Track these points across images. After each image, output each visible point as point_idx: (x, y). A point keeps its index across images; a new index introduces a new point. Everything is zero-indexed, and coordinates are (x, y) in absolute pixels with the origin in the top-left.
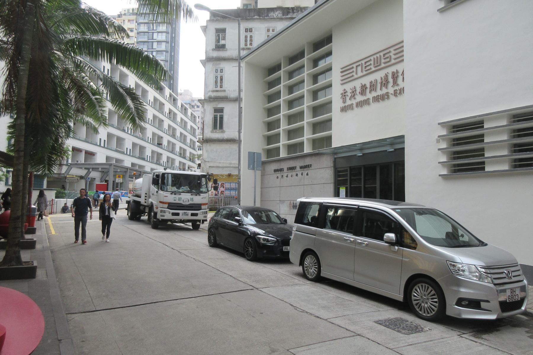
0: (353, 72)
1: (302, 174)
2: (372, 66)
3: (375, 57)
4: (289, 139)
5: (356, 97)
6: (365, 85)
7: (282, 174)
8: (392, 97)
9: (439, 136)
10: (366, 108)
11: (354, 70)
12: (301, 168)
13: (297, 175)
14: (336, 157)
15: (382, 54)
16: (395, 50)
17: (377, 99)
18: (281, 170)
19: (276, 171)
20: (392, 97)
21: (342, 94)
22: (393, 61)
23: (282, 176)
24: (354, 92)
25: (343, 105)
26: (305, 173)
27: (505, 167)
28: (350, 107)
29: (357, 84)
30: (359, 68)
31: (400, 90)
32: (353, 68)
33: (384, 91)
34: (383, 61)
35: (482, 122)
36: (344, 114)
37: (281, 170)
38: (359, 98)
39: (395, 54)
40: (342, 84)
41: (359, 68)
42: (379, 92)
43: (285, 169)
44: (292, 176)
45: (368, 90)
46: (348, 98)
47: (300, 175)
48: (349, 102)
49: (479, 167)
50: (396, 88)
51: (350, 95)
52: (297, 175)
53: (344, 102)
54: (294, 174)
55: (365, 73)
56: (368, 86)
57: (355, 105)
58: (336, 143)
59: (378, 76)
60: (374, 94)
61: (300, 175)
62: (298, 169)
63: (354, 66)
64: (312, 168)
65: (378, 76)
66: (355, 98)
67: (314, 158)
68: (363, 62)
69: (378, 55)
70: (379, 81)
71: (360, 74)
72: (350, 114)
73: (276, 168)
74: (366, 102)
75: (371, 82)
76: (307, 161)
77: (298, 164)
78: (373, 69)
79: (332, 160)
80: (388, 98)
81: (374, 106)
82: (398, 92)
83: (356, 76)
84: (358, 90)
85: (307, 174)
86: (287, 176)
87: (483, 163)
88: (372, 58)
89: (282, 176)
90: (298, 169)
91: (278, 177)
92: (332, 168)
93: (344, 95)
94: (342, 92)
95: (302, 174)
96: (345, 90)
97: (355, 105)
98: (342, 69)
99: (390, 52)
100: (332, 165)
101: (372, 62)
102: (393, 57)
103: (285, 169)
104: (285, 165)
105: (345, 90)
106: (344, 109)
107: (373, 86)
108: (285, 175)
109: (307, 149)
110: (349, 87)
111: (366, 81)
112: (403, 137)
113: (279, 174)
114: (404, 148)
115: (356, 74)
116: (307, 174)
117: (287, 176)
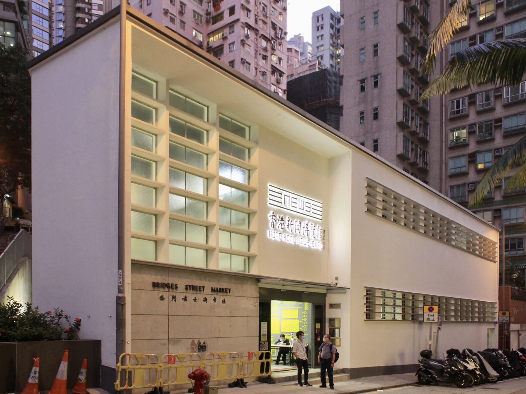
1: (215, 300)
7: (174, 294)
12: (213, 290)
13: (205, 300)
18: (169, 286)
19: (155, 285)
23: (174, 297)
37: (169, 286)
44: (195, 300)
52: (205, 300)
54: (200, 297)
62: (208, 290)
64: (231, 294)
79: (257, 289)
85: (224, 302)
86: (185, 299)
89: (174, 297)
90: (208, 290)
91: (162, 298)
95: (215, 300)
108: (180, 297)
113: (166, 293)
116: (224, 302)
117: (185, 299)
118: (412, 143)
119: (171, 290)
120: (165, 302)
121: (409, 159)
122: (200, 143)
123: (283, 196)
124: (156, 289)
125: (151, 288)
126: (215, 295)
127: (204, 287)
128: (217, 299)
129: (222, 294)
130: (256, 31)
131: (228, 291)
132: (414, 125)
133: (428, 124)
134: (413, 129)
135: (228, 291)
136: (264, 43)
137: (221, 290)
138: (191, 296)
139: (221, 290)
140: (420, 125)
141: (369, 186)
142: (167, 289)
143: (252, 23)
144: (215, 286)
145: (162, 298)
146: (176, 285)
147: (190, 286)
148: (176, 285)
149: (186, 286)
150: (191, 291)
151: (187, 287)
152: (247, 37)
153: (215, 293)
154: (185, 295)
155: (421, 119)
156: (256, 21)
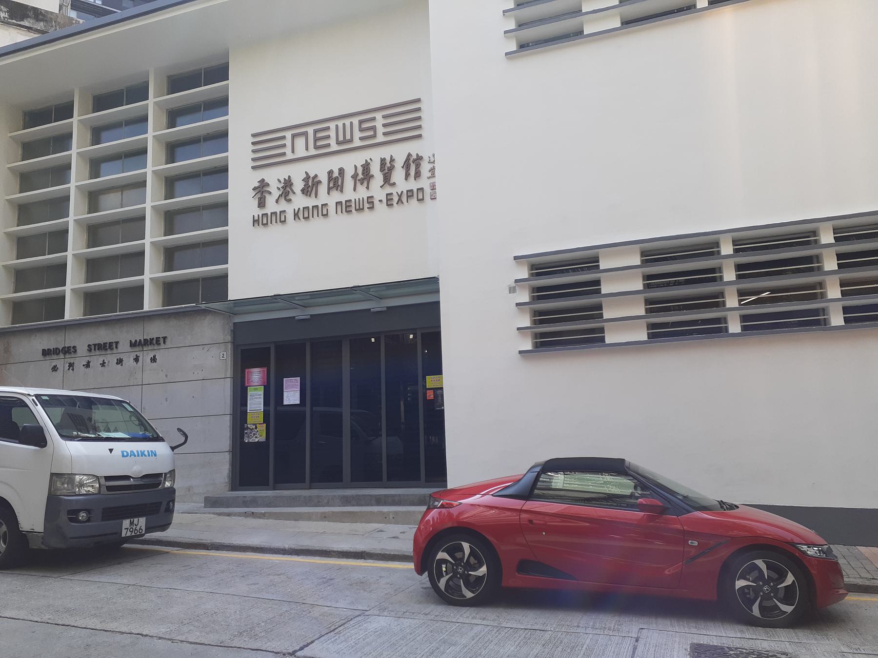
0: (284, 146)
1: (136, 360)
2: (332, 141)
3: (340, 123)
4: (89, 279)
5: (291, 196)
6: (316, 176)
8: (381, 208)
9: (516, 281)
10: (317, 222)
11: (288, 142)
12: (133, 345)
13: (120, 362)
14: (238, 320)
15: (356, 121)
16: (384, 117)
17: (346, 207)
18: (68, 351)
19: (46, 353)
20: (381, 208)
21: (254, 189)
22: (380, 138)
23: (71, 365)
24: (287, 186)
25: (260, 212)
26: (146, 356)
27: (642, 335)
28: (280, 218)
29: (297, 174)
30: (300, 142)
31: (400, 196)
32: (284, 138)
33: (363, 193)
34: (357, 134)
35: (596, 260)
36: (260, 230)
38: (300, 201)
39: (384, 125)
40: (253, 168)
41: (300, 142)
42: (349, 193)
43: (82, 349)
45: (323, 189)
46: (270, 201)
47: (129, 361)
48: (271, 206)
49: (592, 339)
50: (389, 190)
51: (276, 193)
52: (120, 362)
53: (262, 204)
54: (111, 359)
55: (313, 152)
56: (324, 178)
57: (290, 215)
58: (235, 292)
59: (350, 162)
60: (336, 196)
61: (129, 361)
62: (124, 346)
63: (288, 134)
65: (350, 162)
66: (289, 201)
67: (173, 322)
68: (310, 130)
69: (347, 122)
70: (349, 172)
71: (301, 152)
72: (275, 229)
73: (52, 346)
74: (322, 211)
75: (330, 173)
76: (154, 330)
77: (125, 336)
78: (334, 147)
80: (372, 208)
81: (338, 221)
82: (396, 198)
83: (289, 156)
84: (298, 185)
85: (154, 360)
86: (88, 365)
87: (602, 330)
88: (332, 125)
89: (71, 365)
90: (124, 346)
91: (55, 369)
92: (230, 346)
93: (261, 189)
94: (257, 185)
95: (136, 360)
96: (263, 180)
97: (290, 215)
98: (254, 135)
99: (374, 119)
100: (229, 338)
101: (332, 133)
102: (380, 130)
103: (82, 349)
104: (81, 341)
105: (263, 180)
107: (336, 182)
108: (80, 363)
109: (151, 302)
110: (274, 176)
111: (320, 168)
112: (434, 281)
113: (61, 362)
114: (438, 303)
115: (293, 152)
116: (154, 360)
117: (88, 365)
119: (67, 356)
120: (60, 373)
124: (48, 358)
125: (42, 358)
126: (137, 351)
127: (117, 343)
128: (140, 359)
129: (150, 348)
131: (162, 341)
135: (162, 341)
137: (147, 343)
138: (96, 361)
139: (147, 343)
142: (62, 356)
144: (139, 337)
145: (55, 369)
146: (74, 347)
147: (95, 345)
148: (74, 347)
149: (89, 346)
150: (98, 352)
151: (90, 348)
153: (137, 349)
154: (88, 358)
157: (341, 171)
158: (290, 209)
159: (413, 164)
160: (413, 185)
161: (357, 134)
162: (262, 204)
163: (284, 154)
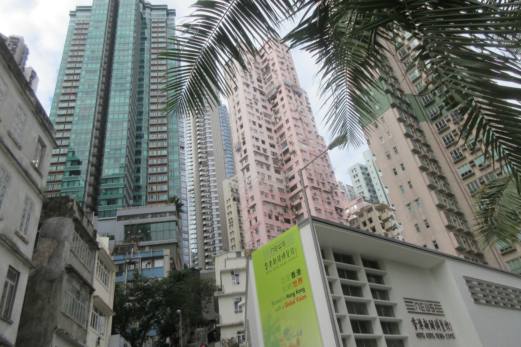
20: (446, 338)
53: (416, 328)
55: (422, 312)
71: (419, 311)
75: (429, 321)
83: (416, 311)
96: (413, 318)
98: (404, 298)
106: (420, 336)
110: (416, 317)
118: (462, 237)
121: (465, 249)
122: (355, 280)
123: (414, 304)
130: (320, 189)
132: (457, 224)
133: (467, 221)
134: (458, 227)
136: (325, 195)
140: (462, 224)
141: (467, 281)
143: (315, 185)
152: (315, 194)
155: (460, 219)
156: (318, 184)
157: (432, 321)
158: (425, 334)
159: (447, 324)
160: (448, 332)
161: (431, 310)
162: (416, 328)
163: (414, 309)
